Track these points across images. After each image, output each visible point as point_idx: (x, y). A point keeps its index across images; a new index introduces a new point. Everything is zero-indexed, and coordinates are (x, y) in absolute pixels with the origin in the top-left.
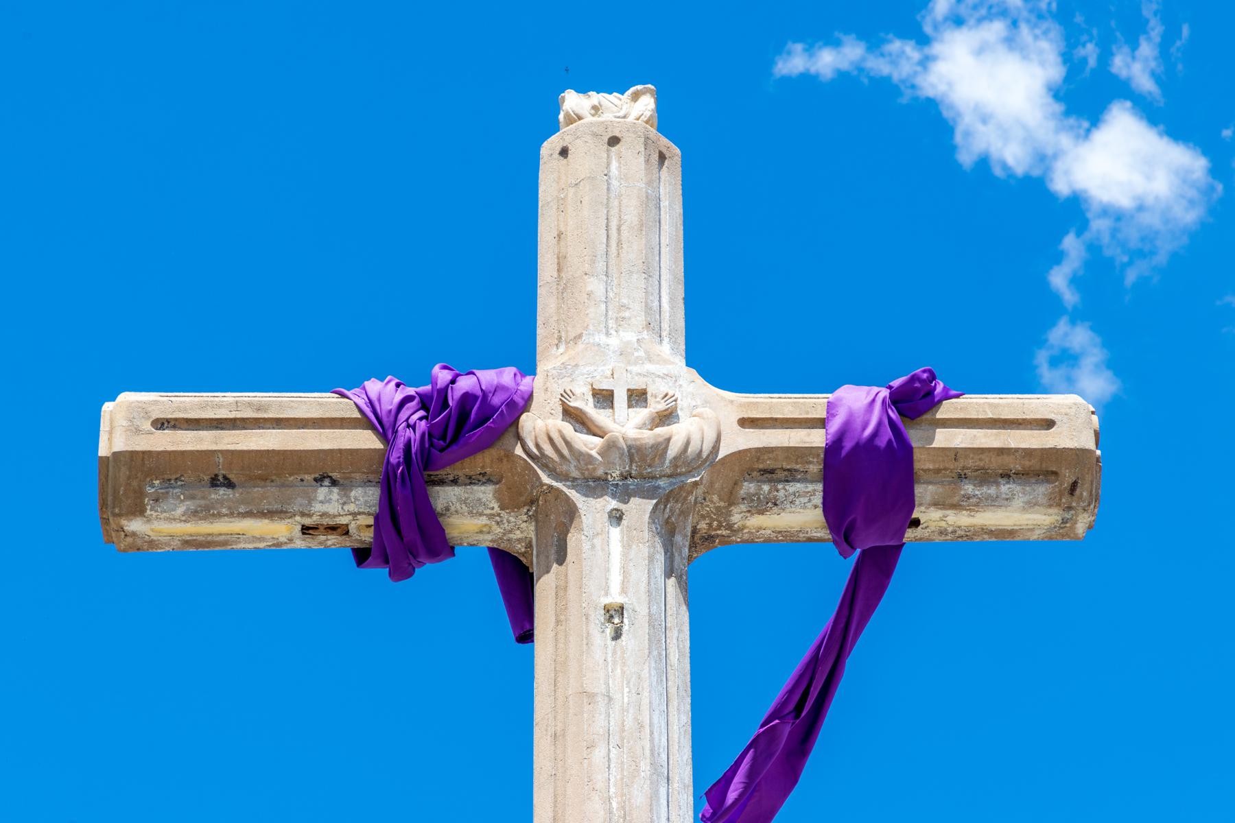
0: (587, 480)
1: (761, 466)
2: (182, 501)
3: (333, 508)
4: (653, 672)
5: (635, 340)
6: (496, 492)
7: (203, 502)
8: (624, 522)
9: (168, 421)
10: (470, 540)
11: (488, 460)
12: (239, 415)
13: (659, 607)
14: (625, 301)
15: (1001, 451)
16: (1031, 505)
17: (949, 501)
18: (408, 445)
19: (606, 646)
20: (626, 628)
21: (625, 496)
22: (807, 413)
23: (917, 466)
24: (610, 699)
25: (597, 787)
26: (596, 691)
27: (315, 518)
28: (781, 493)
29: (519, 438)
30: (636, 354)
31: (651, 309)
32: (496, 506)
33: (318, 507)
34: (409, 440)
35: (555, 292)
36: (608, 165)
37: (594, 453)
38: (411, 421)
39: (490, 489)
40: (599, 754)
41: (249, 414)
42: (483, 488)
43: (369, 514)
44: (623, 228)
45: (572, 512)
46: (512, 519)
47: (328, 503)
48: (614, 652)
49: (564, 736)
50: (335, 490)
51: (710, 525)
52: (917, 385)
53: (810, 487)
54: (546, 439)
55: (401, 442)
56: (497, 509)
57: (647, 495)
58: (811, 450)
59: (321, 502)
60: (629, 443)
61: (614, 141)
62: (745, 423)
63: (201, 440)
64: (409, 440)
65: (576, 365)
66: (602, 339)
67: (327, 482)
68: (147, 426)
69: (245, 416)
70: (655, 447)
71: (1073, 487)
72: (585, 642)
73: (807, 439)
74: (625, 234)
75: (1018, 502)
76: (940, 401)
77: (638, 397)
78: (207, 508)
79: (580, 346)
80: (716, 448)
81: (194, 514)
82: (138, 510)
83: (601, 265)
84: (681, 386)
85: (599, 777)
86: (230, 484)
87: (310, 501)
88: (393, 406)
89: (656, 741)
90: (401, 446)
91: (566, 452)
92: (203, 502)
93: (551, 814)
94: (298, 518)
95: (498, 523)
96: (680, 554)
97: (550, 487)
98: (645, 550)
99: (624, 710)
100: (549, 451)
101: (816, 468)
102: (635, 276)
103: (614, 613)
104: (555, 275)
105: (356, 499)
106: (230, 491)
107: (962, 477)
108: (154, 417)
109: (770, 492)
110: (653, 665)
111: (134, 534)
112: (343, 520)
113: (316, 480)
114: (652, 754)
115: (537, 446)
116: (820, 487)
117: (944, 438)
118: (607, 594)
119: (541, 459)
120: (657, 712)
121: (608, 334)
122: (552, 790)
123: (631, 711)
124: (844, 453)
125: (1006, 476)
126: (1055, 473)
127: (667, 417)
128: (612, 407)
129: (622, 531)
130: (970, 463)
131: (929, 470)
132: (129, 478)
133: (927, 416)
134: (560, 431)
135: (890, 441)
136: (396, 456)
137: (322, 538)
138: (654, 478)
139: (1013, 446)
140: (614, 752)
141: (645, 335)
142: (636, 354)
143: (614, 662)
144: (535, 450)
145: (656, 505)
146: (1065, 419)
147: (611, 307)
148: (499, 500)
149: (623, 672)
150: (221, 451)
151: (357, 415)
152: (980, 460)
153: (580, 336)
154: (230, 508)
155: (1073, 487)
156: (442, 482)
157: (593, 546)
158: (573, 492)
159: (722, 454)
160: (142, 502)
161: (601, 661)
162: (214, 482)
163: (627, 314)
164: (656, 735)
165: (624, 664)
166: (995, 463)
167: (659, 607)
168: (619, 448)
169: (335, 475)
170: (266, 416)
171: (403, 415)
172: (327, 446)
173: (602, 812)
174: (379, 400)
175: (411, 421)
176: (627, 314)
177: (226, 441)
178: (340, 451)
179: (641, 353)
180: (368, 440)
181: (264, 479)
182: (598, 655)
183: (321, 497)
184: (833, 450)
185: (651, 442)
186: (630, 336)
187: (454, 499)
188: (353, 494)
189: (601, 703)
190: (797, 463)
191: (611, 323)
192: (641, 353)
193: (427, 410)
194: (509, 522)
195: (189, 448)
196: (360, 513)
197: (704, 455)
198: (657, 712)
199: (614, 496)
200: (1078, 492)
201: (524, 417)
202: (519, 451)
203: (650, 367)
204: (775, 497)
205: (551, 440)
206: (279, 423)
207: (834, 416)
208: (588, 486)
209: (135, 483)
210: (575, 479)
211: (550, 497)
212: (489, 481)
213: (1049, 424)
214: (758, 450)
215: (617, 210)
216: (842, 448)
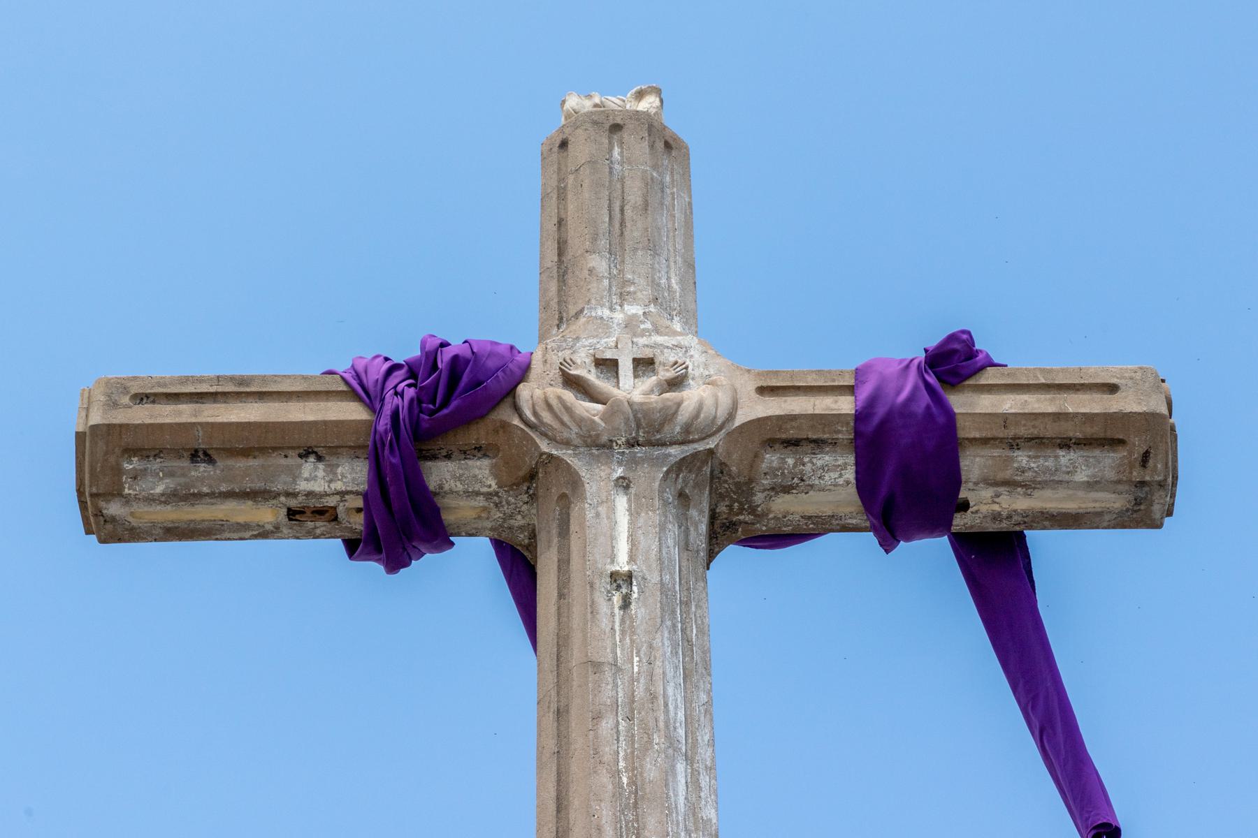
1: (784, 436)
2: (161, 479)
3: (318, 486)
4: (667, 643)
5: (641, 313)
6: (494, 467)
7: (182, 480)
8: (633, 491)
10: (468, 528)
11: (482, 433)
12: (220, 389)
13: (672, 575)
14: (629, 276)
15: (1058, 417)
17: (1001, 476)
18: (395, 414)
19: (613, 615)
20: (635, 596)
21: (633, 462)
22: (834, 380)
24: (619, 670)
25: (605, 759)
26: (602, 660)
27: (300, 498)
28: (808, 467)
29: (517, 409)
30: (642, 326)
31: (659, 285)
32: (493, 483)
33: (303, 486)
34: (397, 407)
35: (555, 275)
36: (611, 150)
37: (596, 419)
38: (400, 388)
39: (486, 462)
40: (606, 725)
42: (478, 463)
43: (357, 493)
44: (626, 207)
45: (575, 483)
46: (512, 500)
47: (314, 479)
48: (623, 621)
49: (567, 711)
50: (321, 466)
51: (730, 507)
52: (957, 346)
54: (544, 406)
55: (387, 410)
56: (494, 486)
57: (655, 462)
58: (839, 417)
59: (306, 479)
60: (636, 407)
61: (616, 128)
62: (762, 390)
63: (180, 413)
64: (397, 407)
65: (578, 339)
66: (606, 313)
67: (312, 459)
69: (227, 389)
70: (664, 409)
71: (1145, 457)
72: (589, 610)
73: (833, 406)
74: (629, 212)
76: (982, 368)
77: (644, 365)
79: (582, 320)
80: (731, 416)
83: (603, 243)
84: (692, 356)
85: (607, 749)
86: (209, 459)
87: (295, 478)
88: (380, 376)
89: (672, 714)
90: (389, 413)
91: (566, 418)
92: (182, 480)
93: (553, 794)
94: (282, 499)
95: (496, 505)
96: (696, 529)
97: (550, 456)
98: (656, 518)
99: (632, 680)
100: (547, 417)
101: (846, 434)
102: (640, 253)
103: (622, 580)
104: (556, 259)
105: (343, 476)
106: (210, 468)
109: (795, 465)
110: (666, 634)
111: (113, 520)
112: (331, 502)
114: (667, 726)
116: (851, 459)
118: (612, 562)
120: (672, 684)
121: (612, 309)
122: (554, 768)
123: (642, 681)
126: (1121, 442)
127: (676, 383)
128: (617, 377)
129: (629, 500)
131: (975, 439)
132: (106, 453)
133: (971, 382)
134: (559, 398)
135: (928, 407)
136: (384, 422)
137: (310, 524)
139: (1071, 410)
140: (623, 725)
141: (652, 308)
142: (642, 326)
143: (623, 632)
144: (533, 419)
145: (667, 472)
146: (1130, 383)
147: (614, 283)
148: (496, 476)
149: (632, 641)
150: (200, 424)
151: (343, 388)
152: (1034, 427)
153: (582, 311)
154: (210, 487)
155: (1145, 457)
156: (434, 457)
157: (598, 515)
158: (576, 461)
159: (740, 419)
160: (120, 480)
161: (608, 630)
162: (195, 456)
163: (632, 289)
164: (671, 707)
165: (633, 633)
166: (1051, 430)
167: (673, 578)
168: (623, 413)
169: (320, 451)
170: (248, 390)
171: (391, 383)
172: (311, 418)
173: (610, 787)
174: (366, 372)
175: (400, 388)
176: (632, 289)
177: (206, 413)
178: (325, 423)
179: (648, 325)
182: (604, 623)
183: (306, 475)
184: (861, 417)
185: (660, 406)
186: (634, 309)
187: (448, 476)
188: (339, 470)
189: (608, 675)
190: (824, 432)
191: (615, 299)
192: (648, 325)
193: (416, 379)
194: (508, 503)
195: (168, 421)
196: (348, 492)
197: (719, 422)
198: (672, 684)
199: (620, 463)
200: (1151, 463)
201: (521, 386)
202: (516, 421)
203: (659, 339)
204: (801, 472)
205: (549, 407)
206: (262, 396)
207: (863, 382)
208: (592, 454)
209: (112, 459)
210: (577, 447)
211: (551, 468)
212: (485, 455)
213: (1112, 388)
214: (779, 417)
215: (620, 192)
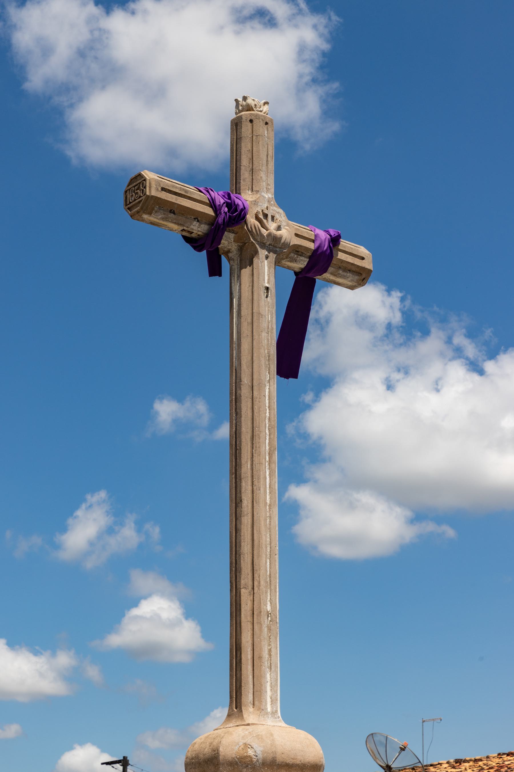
0: (261, 242)
9: (164, 188)
15: (353, 264)
16: (352, 281)
23: (333, 262)
29: (246, 223)
32: (233, 240)
33: (192, 227)
41: (183, 193)
53: (306, 259)
67: (196, 220)
68: (160, 189)
75: (349, 279)
78: (166, 218)
81: (163, 219)
82: (150, 214)
86: (174, 213)
87: (191, 224)
101: (309, 254)
107: (340, 268)
108: (162, 186)
113: (194, 219)
115: (251, 228)
116: (308, 260)
117: (341, 256)
119: (251, 232)
124: (318, 253)
125: (350, 271)
126: (361, 274)
130: (344, 265)
138: (276, 247)
148: (234, 238)
169: (199, 219)
172: (202, 210)
177: (178, 201)
180: (210, 211)
181: (182, 214)
202: (245, 228)
212: (233, 233)
214: (299, 245)
216: (318, 251)
